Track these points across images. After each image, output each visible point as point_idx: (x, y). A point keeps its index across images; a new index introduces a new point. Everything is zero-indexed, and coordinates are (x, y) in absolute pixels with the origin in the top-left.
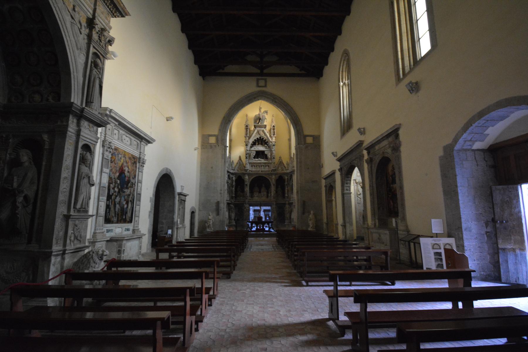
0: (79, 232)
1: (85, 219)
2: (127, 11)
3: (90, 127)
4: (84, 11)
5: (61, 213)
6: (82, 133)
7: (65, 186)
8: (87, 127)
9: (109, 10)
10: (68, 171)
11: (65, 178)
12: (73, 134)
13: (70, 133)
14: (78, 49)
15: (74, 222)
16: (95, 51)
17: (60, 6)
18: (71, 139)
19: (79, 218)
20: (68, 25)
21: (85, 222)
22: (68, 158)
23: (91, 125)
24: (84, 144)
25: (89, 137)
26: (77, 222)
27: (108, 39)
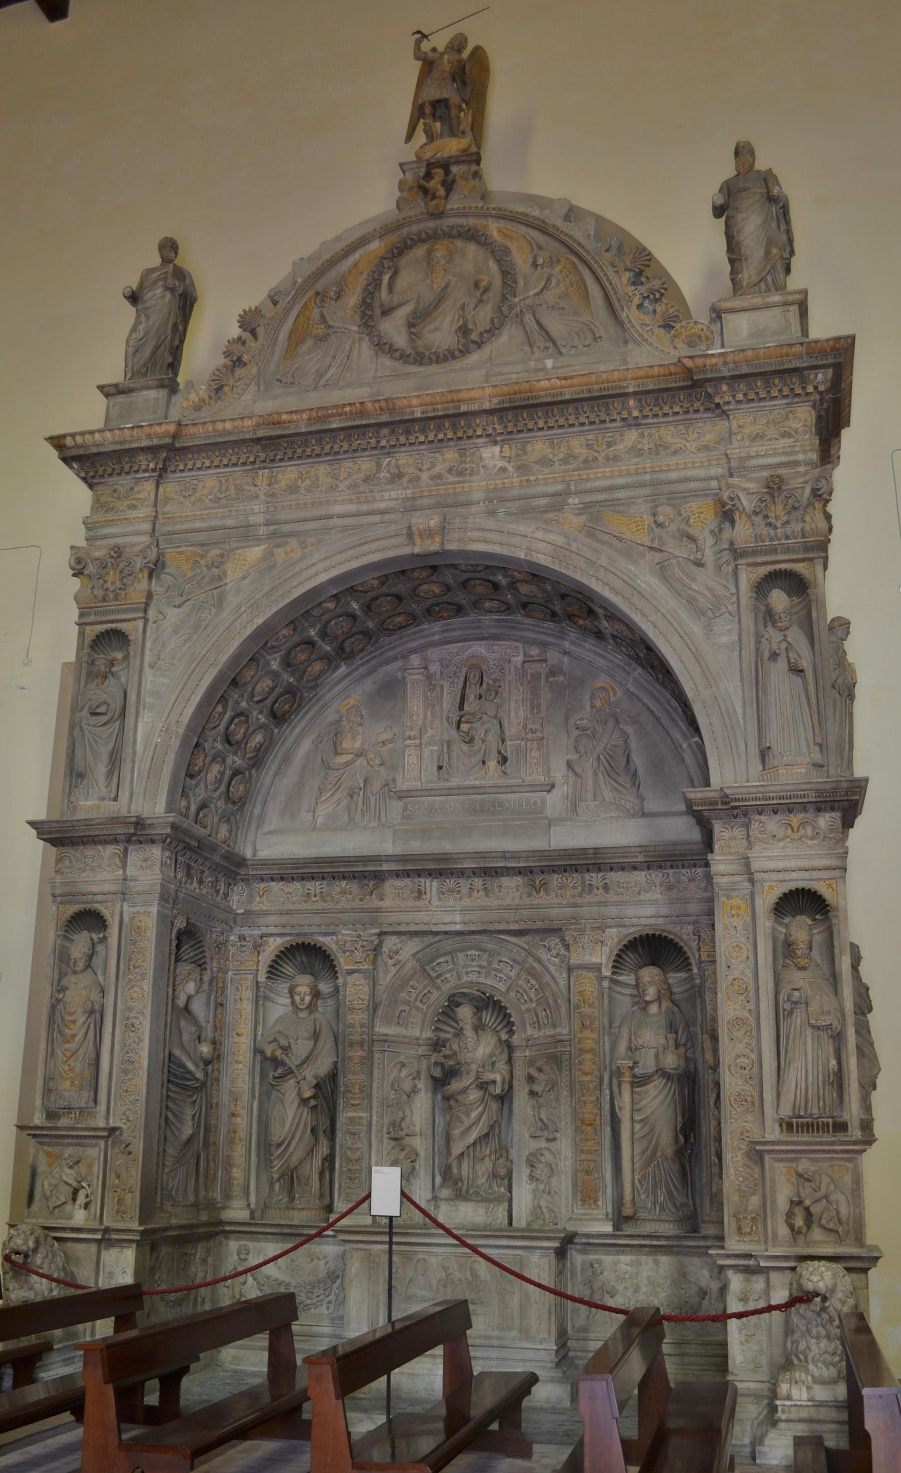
0: (826, 1197)
1: (851, 1155)
2: (827, 340)
3: (792, 829)
4: (695, 494)
5: (742, 1133)
6: (755, 866)
7: (740, 1048)
8: (780, 833)
9: (785, 401)
10: (743, 997)
11: (738, 1022)
12: (737, 878)
13: (725, 880)
14: (699, 612)
15: (794, 1165)
16: (763, 571)
17: (603, 561)
18: (734, 894)
19: (814, 1151)
20: (648, 581)
21: (850, 1165)
22: (737, 957)
23: (795, 819)
24: (785, 894)
25: (793, 864)
26: (804, 1165)
27: (808, 491)
